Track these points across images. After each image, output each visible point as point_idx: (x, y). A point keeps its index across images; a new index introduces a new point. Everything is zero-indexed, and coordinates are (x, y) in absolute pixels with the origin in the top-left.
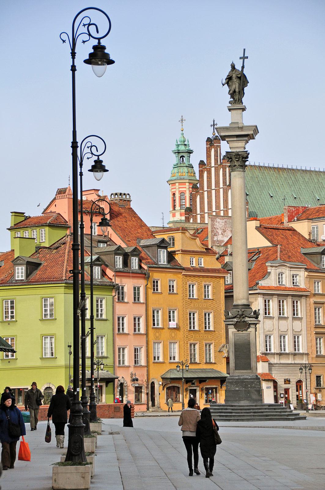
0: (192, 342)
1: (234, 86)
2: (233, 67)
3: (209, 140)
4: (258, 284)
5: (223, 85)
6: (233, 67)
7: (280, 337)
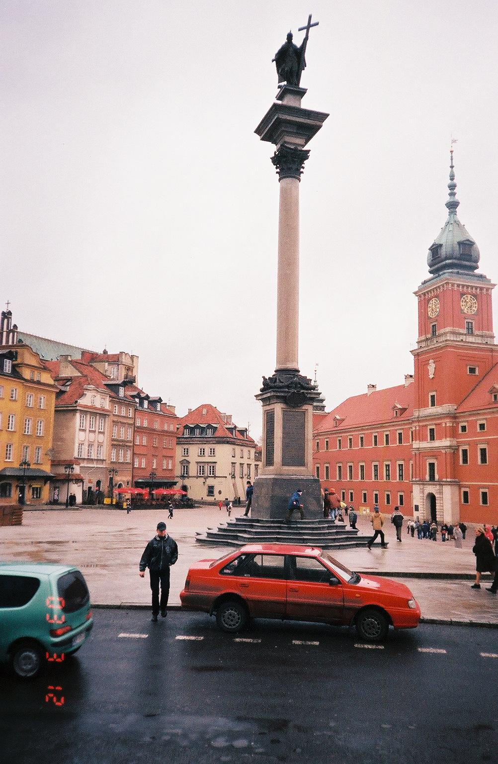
0: (25, 444)
1: (289, 64)
2: (290, 37)
3: (3, 313)
4: (76, 402)
5: (273, 61)
6: (290, 37)
7: (89, 445)
